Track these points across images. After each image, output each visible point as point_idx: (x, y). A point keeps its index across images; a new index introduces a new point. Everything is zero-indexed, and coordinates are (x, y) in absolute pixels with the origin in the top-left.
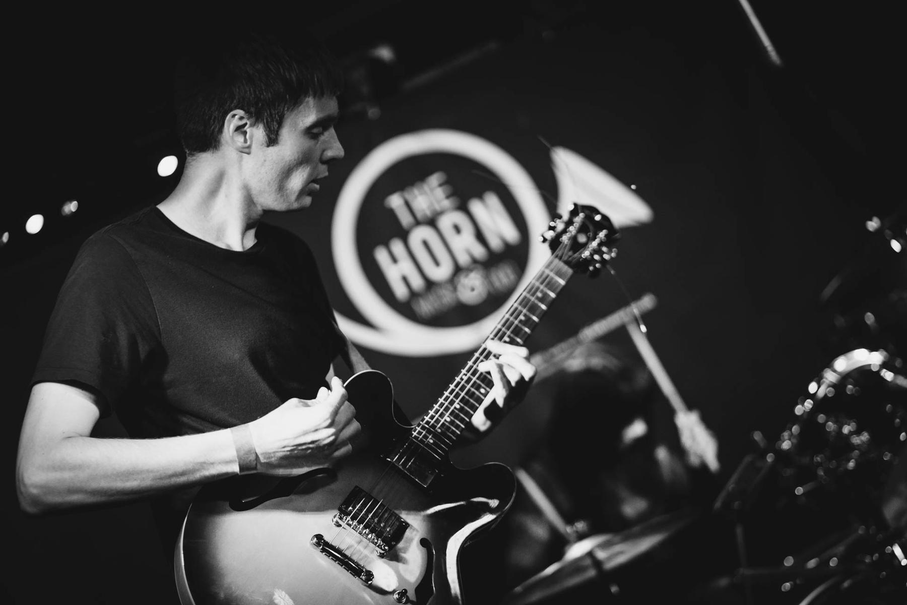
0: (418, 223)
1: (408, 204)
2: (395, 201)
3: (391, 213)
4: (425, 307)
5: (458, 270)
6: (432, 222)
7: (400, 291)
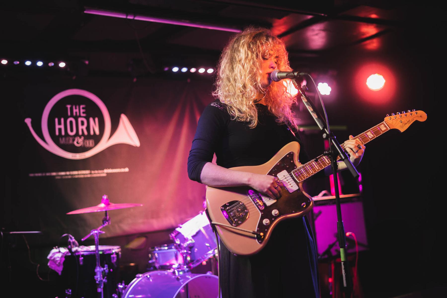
0: (72, 116)
2: (69, 106)
4: (62, 141)
5: (77, 134)
6: (76, 118)
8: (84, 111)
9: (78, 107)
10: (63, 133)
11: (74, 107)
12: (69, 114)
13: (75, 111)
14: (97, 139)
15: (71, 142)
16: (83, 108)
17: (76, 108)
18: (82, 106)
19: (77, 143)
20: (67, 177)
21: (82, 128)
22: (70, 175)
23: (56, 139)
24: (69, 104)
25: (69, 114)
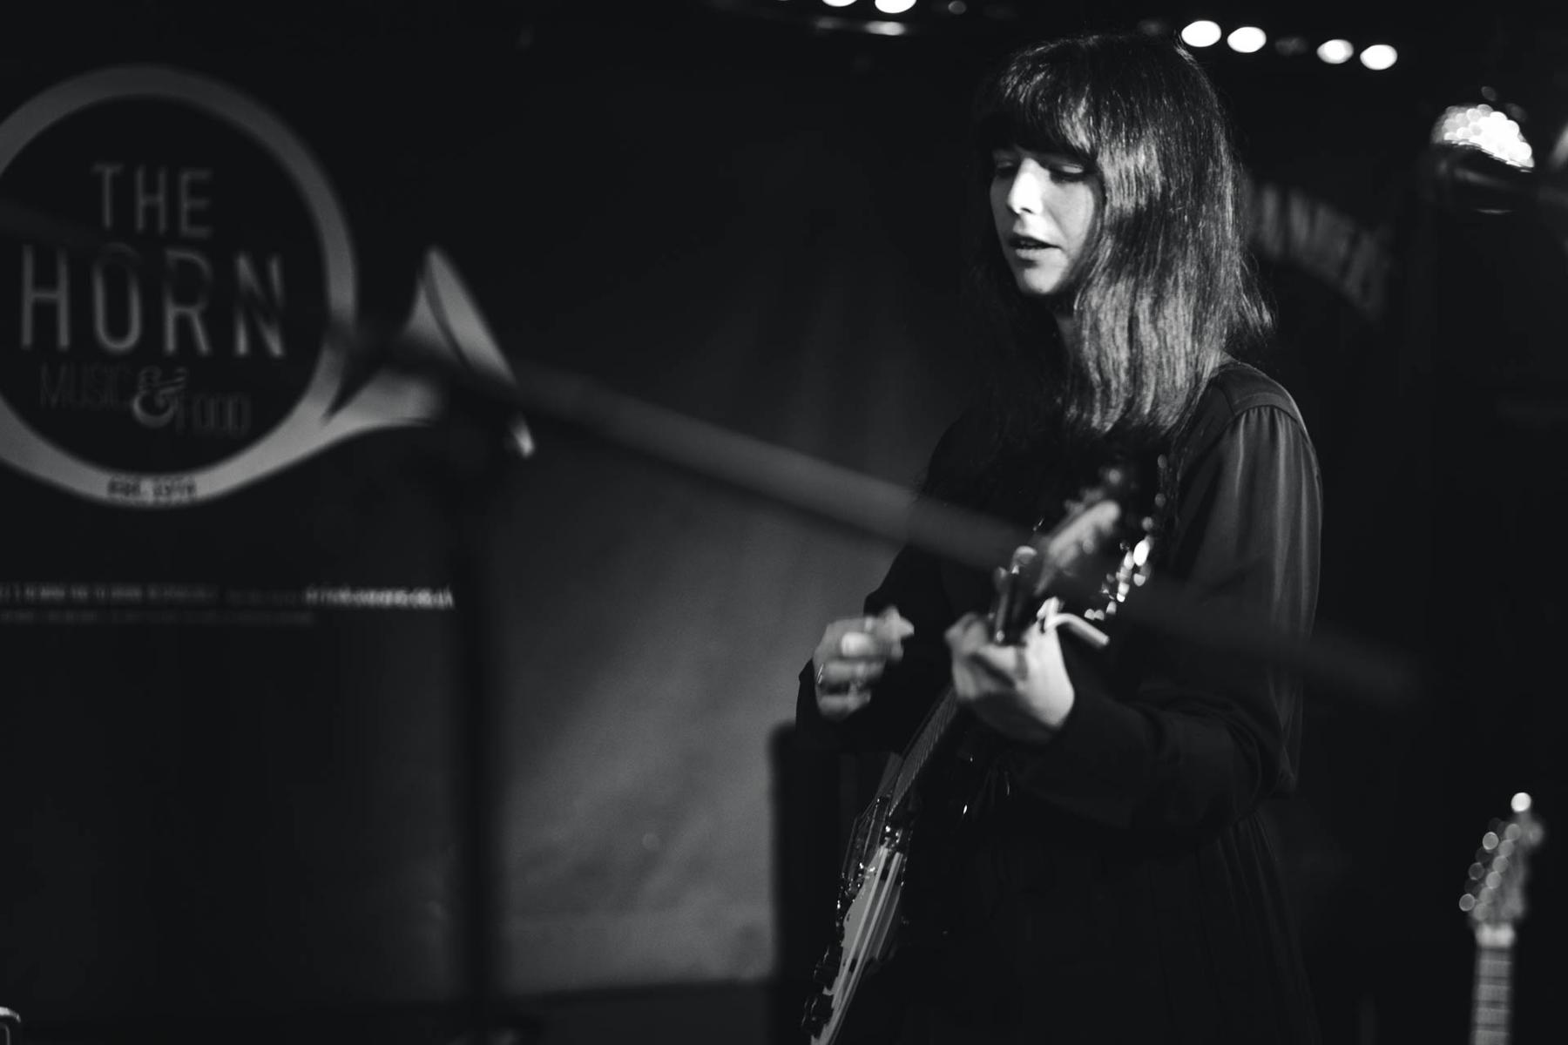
1: (124, 188)
8: (202, 203)
9: (162, 178)
10: (64, 340)
11: (140, 176)
12: (108, 220)
13: (142, 202)
16: (196, 190)
19: (148, 405)
20: (70, 617)
22: (91, 604)
25: (108, 220)
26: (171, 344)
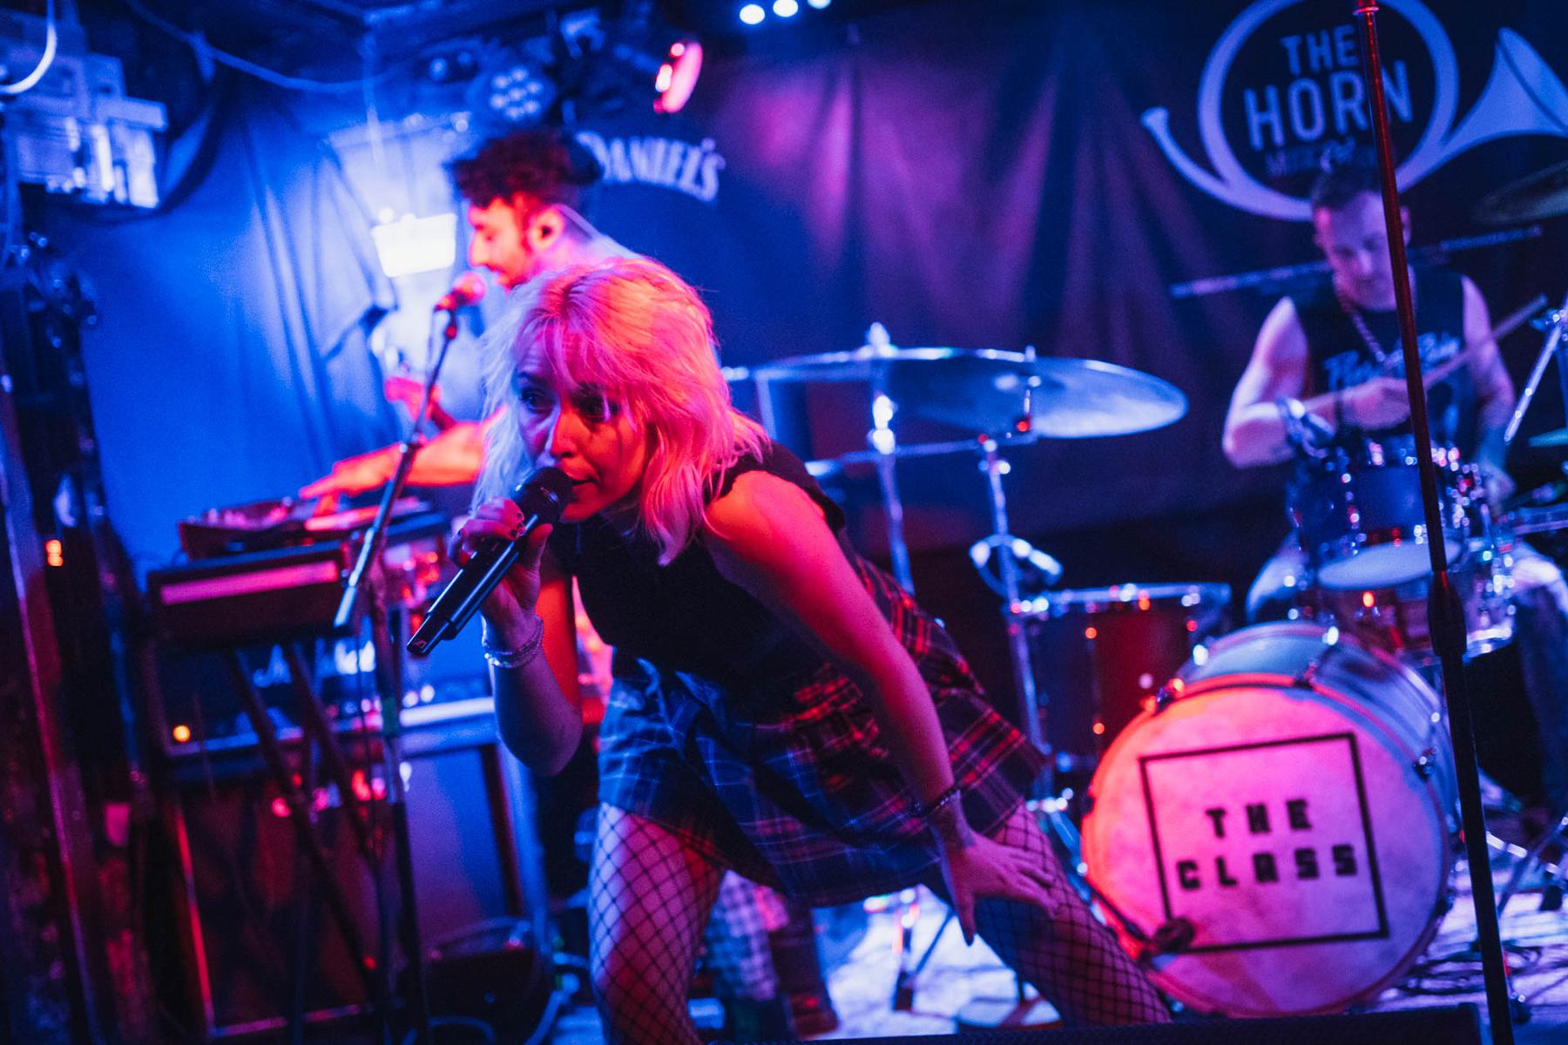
0: (1306, 72)
1: (1303, 51)
2: (1291, 43)
3: (1284, 53)
5: (1330, 132)
6: (1322, 79)
7: (1257, 140)
8: (1350, 45)
9: (1325, 38)
10: (1278, 137)
11: (1311, 40)
13: (1314, 52)
14: (1408, 137)
15: (1309, 162)
16: (1346, 38)
17: (1319, 43)
18: (1339, 32)
21: (1350, 108)
23: (1254, 164)
24: (1290, 34)
26: (1341, 124)
